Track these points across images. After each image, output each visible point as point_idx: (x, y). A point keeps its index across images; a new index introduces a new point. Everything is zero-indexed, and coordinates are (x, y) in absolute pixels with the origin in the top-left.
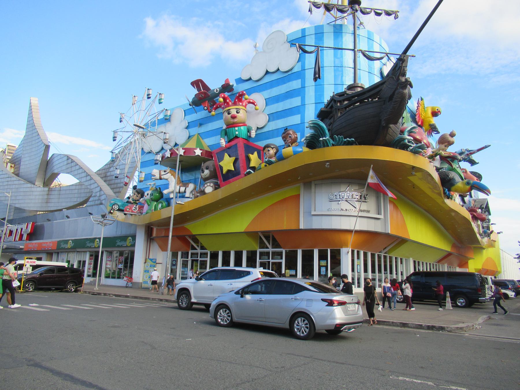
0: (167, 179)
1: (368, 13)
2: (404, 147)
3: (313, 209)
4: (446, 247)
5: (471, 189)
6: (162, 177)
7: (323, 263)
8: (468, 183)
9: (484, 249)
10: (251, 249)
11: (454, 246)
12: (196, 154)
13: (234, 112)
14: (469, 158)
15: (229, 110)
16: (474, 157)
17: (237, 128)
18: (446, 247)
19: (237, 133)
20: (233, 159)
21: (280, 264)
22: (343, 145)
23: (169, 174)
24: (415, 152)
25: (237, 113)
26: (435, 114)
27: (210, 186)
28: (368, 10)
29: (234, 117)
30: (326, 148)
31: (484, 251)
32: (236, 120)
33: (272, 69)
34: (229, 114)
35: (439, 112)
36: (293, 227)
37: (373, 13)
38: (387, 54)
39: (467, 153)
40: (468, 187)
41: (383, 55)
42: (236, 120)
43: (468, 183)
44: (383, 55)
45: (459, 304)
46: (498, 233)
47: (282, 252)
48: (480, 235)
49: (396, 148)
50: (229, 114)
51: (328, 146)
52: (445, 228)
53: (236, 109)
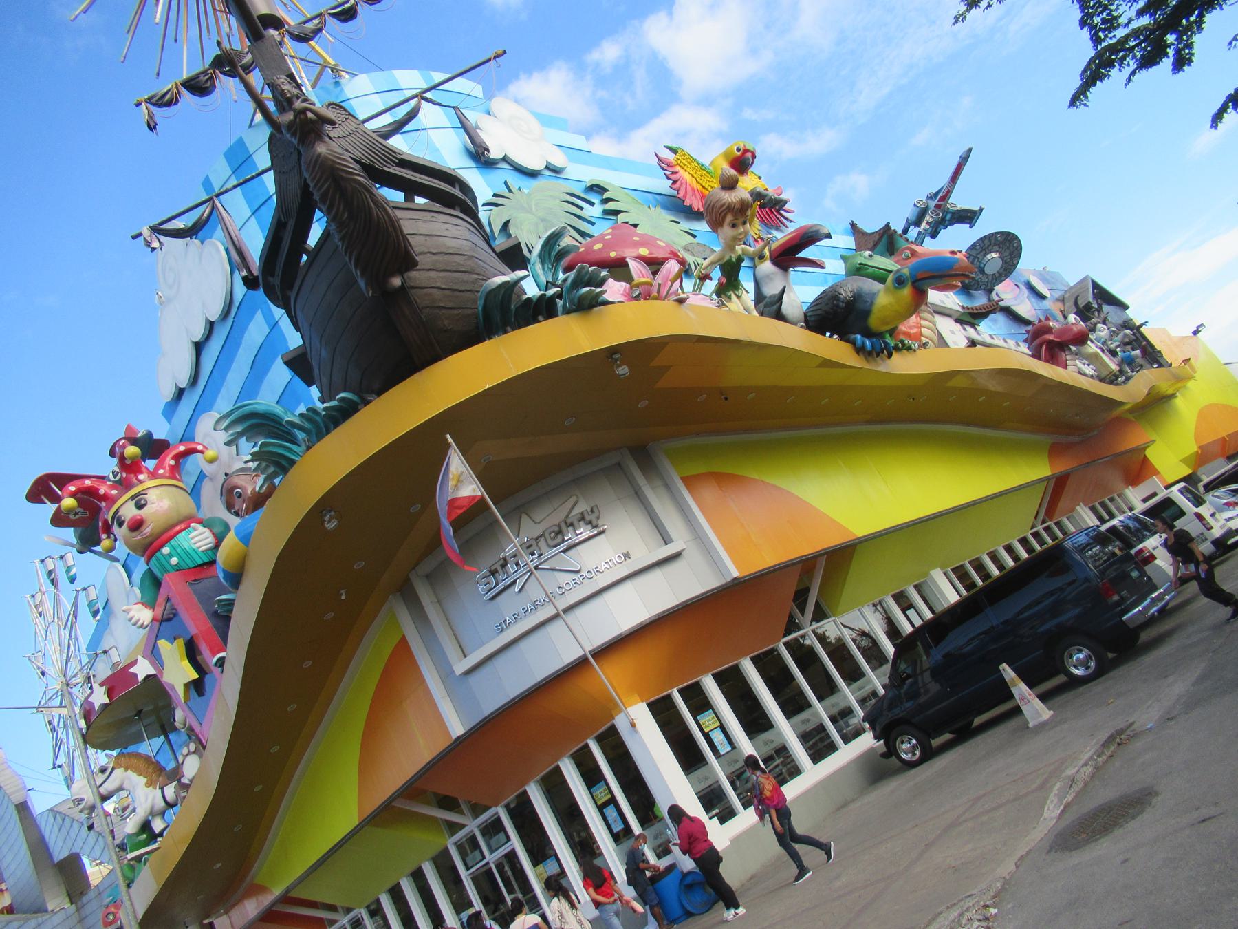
0: (120, 789)
1: (318, 31)
2: (542, 309)
3: (451, 651)
4: (1038, 469)
5: (920, 296)
6: (102, 790)
7: (600, 791)
8: (900, 282)
9: (1173, 396)
10: (435, 850)
11: (1055, 451)
12: (141, 678)
13: (129, 511)
14: (946, 211)
15: (117, 512)
16: (959, 201)
17: (166, 550)
18: (1038, 469)
19: (174, 561)
20: (180, 643)
21: (512, 857)
22: (328, 432)
23: (119, 772)
24: (587, 305)
25: (140, 506)
26: (742, 163)
27: (189, 753)
28: (310, 25)
29: (137, 525)
30: (293, 471)
31: (1179, 402)
32: (147, 530)
33: (198, 335)
34: (121, 524)
35: (746, 151)
36: (441, 745)
37: (332, 23)
38: (421, 96)
39: (932, 204)
40: (907, 291)
41: (413, 103)
42: (147, 530)
43: (900, 282)
44: (413, 103)
45: (1079, 672)
46: (1195, 333)
47: (498, 821)
48: (1111, 379)
49: (505, 332)
50: (121, 524)
51: (293, 463)
52: (989, 427)
53: (133, 498)
